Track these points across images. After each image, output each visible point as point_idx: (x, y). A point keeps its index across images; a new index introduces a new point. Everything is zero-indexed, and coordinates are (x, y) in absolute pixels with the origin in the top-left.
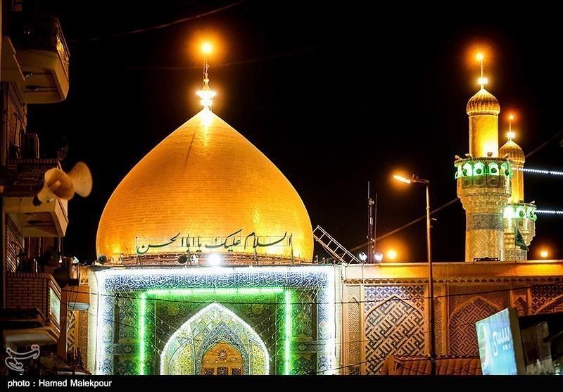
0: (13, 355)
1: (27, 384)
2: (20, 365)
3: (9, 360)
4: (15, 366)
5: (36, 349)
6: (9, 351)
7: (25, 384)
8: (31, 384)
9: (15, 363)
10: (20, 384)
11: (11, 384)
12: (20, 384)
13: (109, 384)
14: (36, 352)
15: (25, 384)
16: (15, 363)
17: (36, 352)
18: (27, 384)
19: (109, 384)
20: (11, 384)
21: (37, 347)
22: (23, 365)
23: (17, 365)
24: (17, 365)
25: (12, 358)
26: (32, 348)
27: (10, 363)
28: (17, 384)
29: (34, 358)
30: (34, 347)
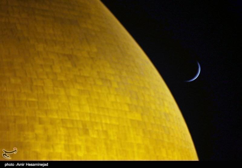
0: (6, 152)
1: (13, 165)
2: (9, 157)
3: (4, 154)
4: (6, 157)
5: (15, 150)
6: (4, 150)
7: (12, 165)
8: (15, 165)
9: (6, 155)
10: (10, 165)
11: (6, 165)
12: (10, 165)
13: (47, 165)
14: (16, 151)
15: (12, 165)
16: (6, 155)
17: (16, 151)
18: (13, 165)
19: (47, 165)
20: (6, 165)
21: (16, 149)
22: (10, 156)
23: (8, 157)
24: (8, 157)
25: (5, 153)
26: (14, 149)
27: (4, 156)
28: (9, 165)
29: (15, 153)
30: (15, 149)
